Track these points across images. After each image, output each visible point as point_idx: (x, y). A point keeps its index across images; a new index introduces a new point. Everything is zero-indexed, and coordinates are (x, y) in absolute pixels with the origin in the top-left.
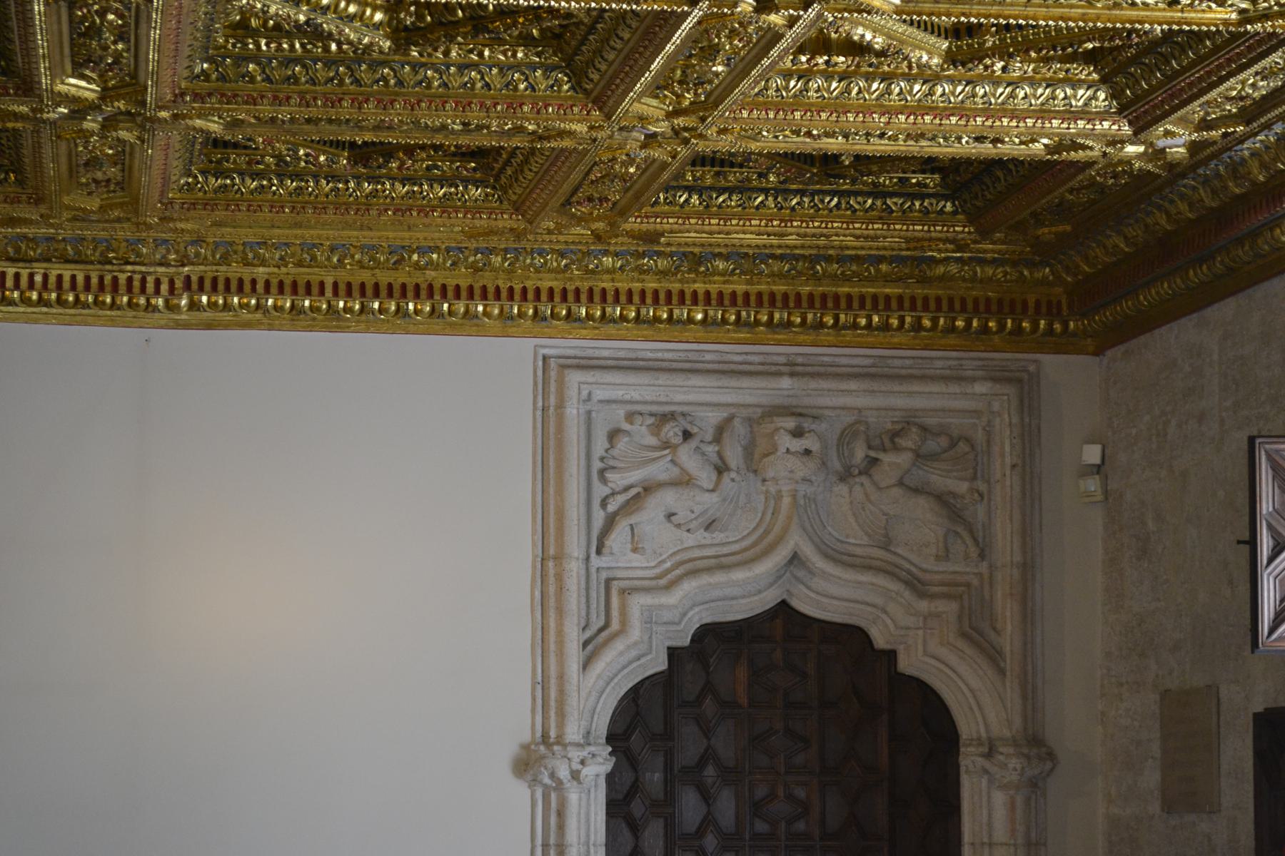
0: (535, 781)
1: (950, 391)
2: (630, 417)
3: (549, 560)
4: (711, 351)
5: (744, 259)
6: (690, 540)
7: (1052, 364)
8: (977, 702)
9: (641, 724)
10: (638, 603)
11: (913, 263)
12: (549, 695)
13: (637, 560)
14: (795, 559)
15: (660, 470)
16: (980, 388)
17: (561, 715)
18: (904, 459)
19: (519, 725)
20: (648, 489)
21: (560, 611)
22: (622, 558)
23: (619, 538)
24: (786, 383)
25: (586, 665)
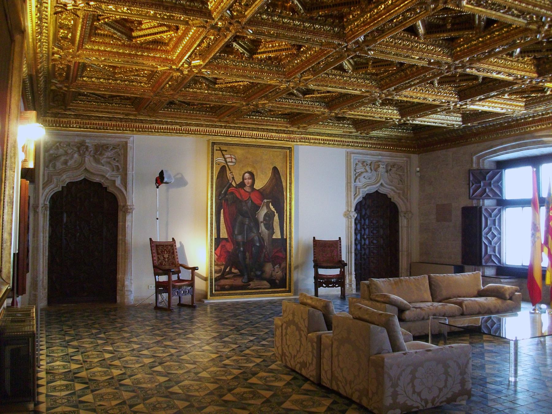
0: (348, 217)
1: (400, 158)
2: (359, 161)
3: (348, 183)
4: (369, 152)
5: (378, 138)
6: (367, 181)
7: (412, 155)
8: (402, 207)
9: (359, 207)
10: (361, 190)
11: (399, 139)
12: (348, 203)
13: (359, 184)
14: (382, 184)
15: (363, 170)
16: (405, 159)
17: (351, 207)
18: (395, 169)
19: (344, 208)
20: (362, 173)
21: (351, 191)
22: (359, 184)
23: (357, 180)
24: (380, 157)
25: (354, 199)
